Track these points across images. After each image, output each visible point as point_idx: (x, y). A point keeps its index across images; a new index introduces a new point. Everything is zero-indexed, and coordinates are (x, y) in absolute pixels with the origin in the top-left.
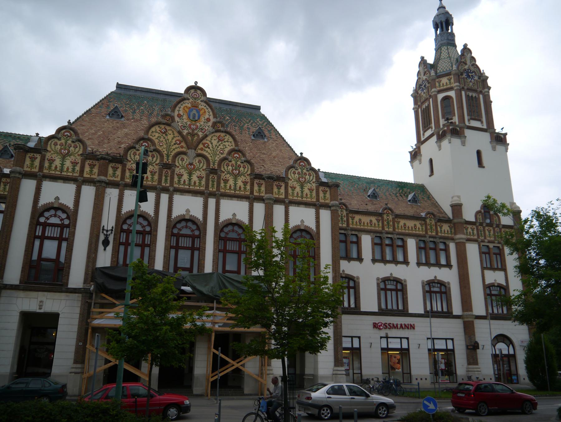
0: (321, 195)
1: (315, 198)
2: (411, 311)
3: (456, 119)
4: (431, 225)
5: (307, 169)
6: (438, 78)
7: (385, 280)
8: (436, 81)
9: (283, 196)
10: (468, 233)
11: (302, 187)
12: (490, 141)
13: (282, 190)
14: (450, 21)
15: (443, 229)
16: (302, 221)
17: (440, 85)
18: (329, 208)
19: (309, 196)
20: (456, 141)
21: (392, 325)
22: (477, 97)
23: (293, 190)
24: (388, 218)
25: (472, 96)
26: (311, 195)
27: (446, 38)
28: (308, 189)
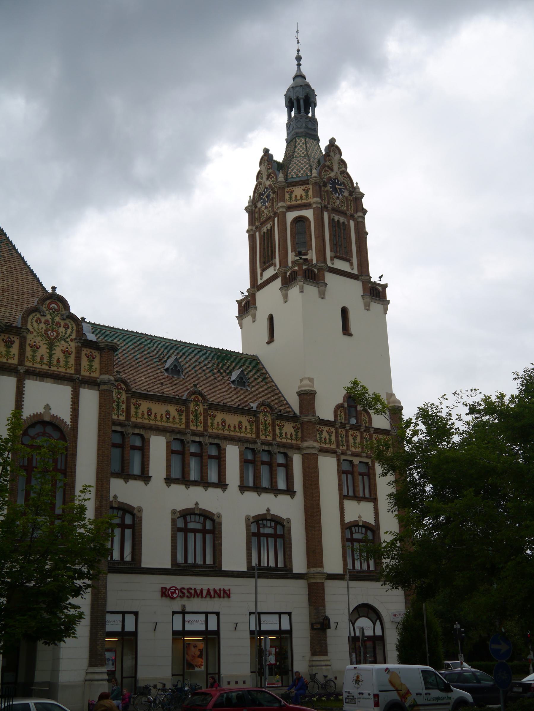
0: (85, 362)
1: (73, 368)
2: (226, 567)
3: (312, 255)
4: (265, 424)
5: (62, 315)
6: (288, 186)
7: (186, 514)
8: (286, 190)
9: (15, 361)
10: (323, 439)
11: (51, 346)
12: (362, 294)
13: (15, 350)
14: (312, 100)
15: (284, 432)
16: (47, 407)
17: (291, 198)
18: (97, 387)
19: (62, 363)
20: (311, 290)
21: (192, 592)
22: (346, 223)
23: (34, 352)
24: (196, 408)
25: (338, 221)
26: (66, 362)
27: (304, 125)
28: (62, 350)
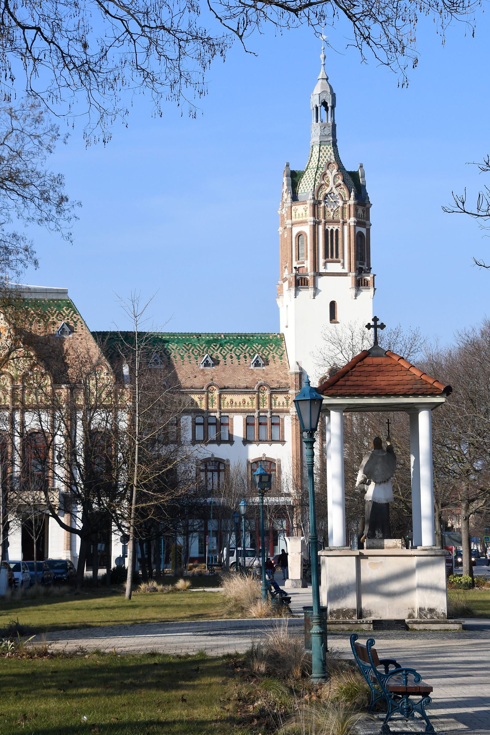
3: (308, 264)
